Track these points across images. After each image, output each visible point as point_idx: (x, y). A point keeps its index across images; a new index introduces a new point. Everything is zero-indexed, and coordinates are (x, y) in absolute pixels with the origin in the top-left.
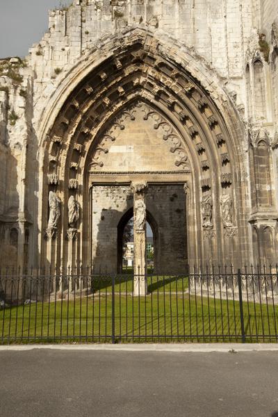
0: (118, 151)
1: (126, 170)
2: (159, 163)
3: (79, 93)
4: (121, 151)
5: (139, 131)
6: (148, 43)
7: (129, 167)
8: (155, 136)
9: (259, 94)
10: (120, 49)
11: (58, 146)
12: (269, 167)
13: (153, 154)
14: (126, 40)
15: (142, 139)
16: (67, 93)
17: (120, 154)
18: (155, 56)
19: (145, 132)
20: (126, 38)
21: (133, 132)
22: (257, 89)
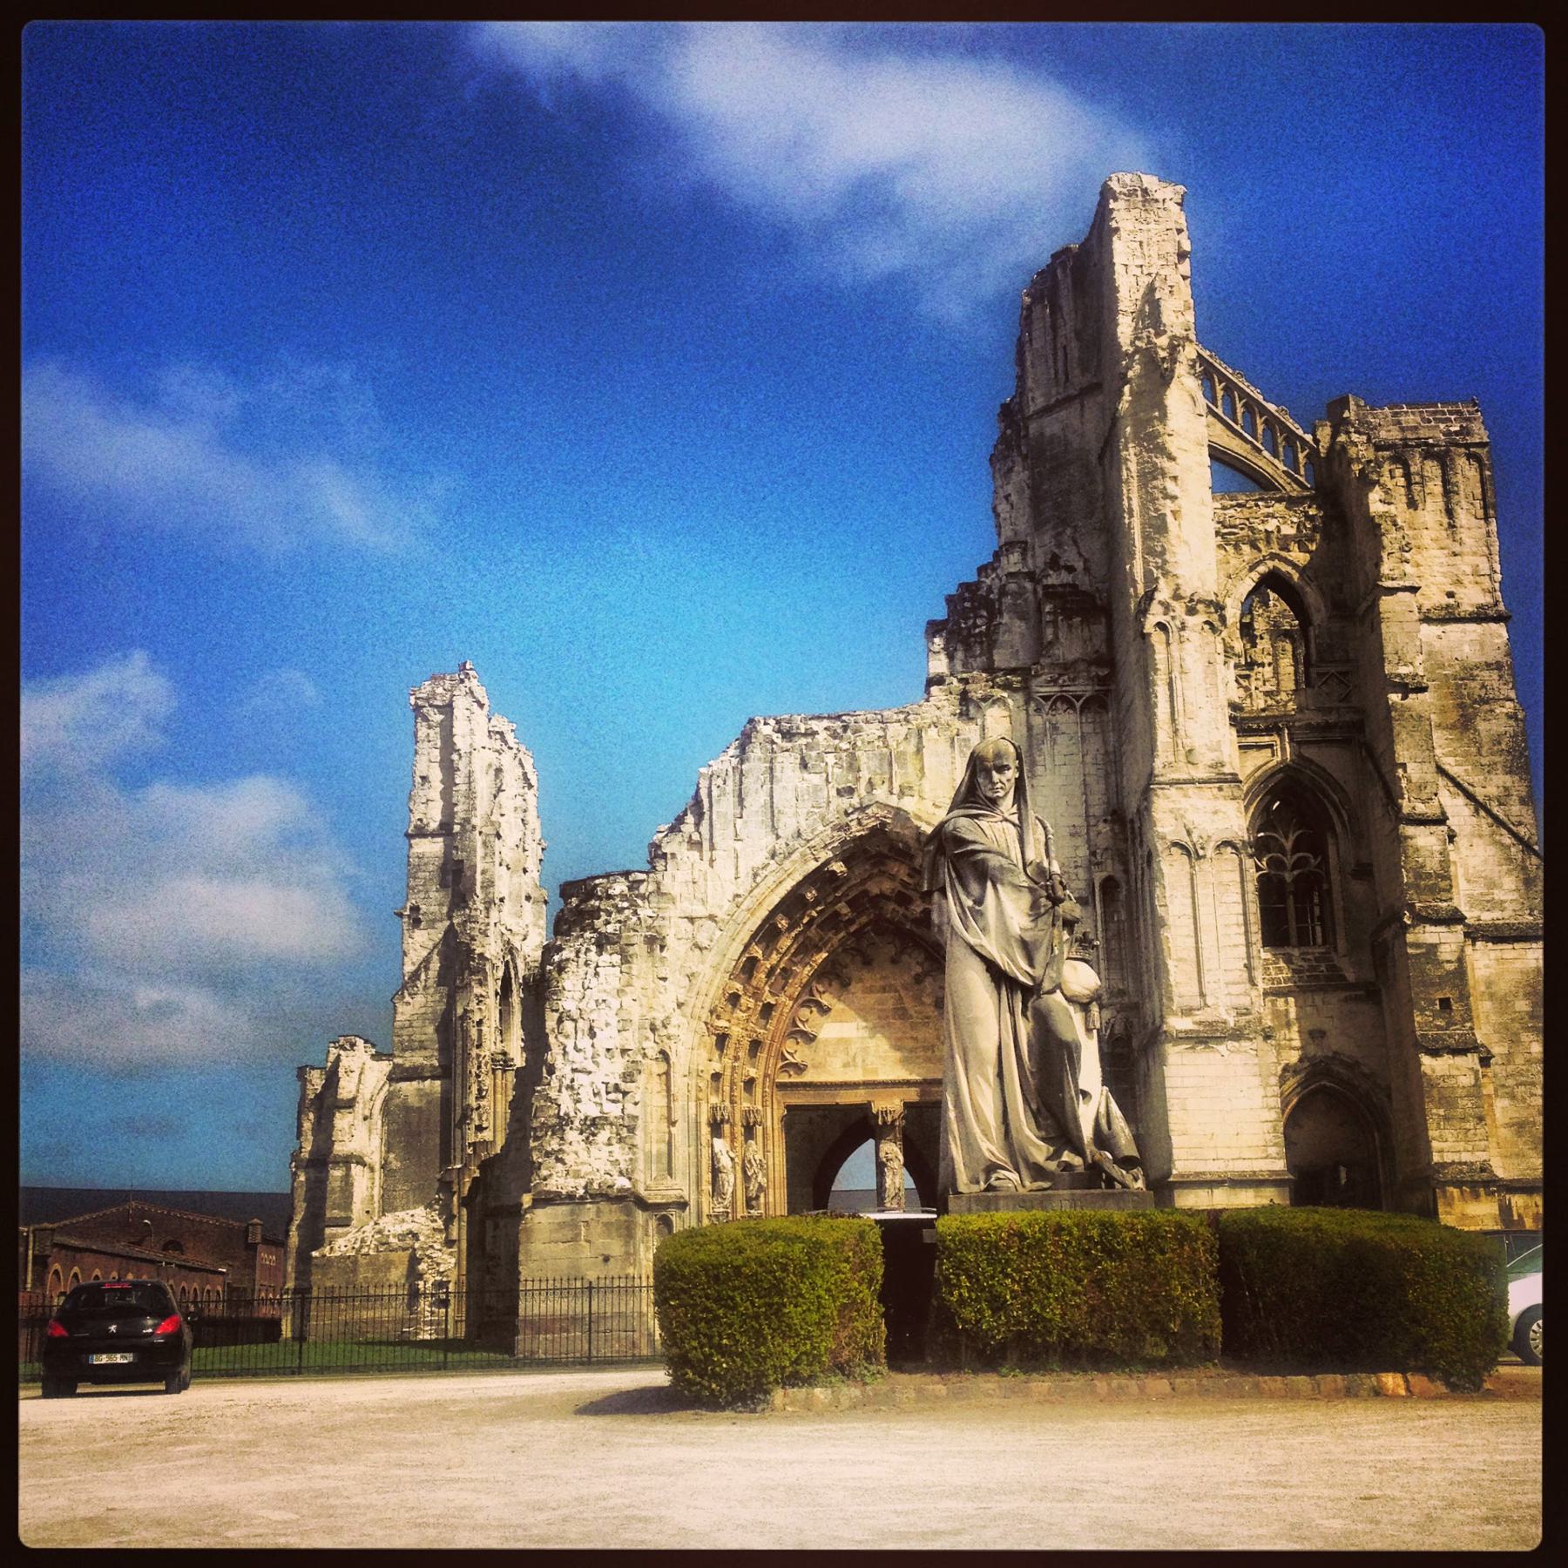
0: (839, 1035)
1: (856, 1076)
2: (929, 1060)
3: (767, 934)
4: (846, 1035)
5: (884, 990)
6: (893, 827)
7: (865, 1069)
8: (918, 999)
9: (1114, 944)
10: (843, 843)
11: (722, 1040)
12: (1133, 1089)
13: (916, 1039)
14: (854, 826)
15: (890, 1004)
16: (745, 936)
17: (844, 1042)
18: (912, 851)
19: (896, 991)
20: (854, 823)
21: (871, 990)
22: (1110, 934)
